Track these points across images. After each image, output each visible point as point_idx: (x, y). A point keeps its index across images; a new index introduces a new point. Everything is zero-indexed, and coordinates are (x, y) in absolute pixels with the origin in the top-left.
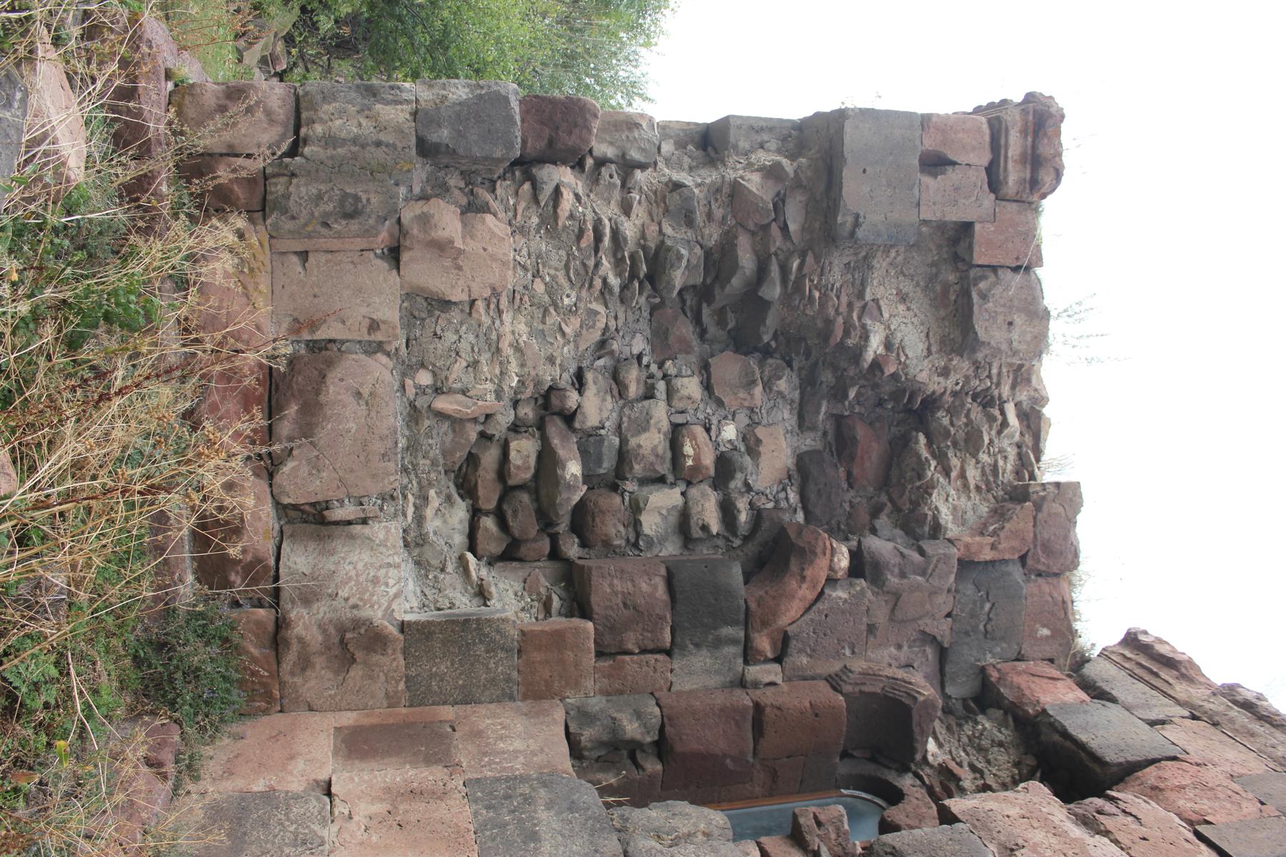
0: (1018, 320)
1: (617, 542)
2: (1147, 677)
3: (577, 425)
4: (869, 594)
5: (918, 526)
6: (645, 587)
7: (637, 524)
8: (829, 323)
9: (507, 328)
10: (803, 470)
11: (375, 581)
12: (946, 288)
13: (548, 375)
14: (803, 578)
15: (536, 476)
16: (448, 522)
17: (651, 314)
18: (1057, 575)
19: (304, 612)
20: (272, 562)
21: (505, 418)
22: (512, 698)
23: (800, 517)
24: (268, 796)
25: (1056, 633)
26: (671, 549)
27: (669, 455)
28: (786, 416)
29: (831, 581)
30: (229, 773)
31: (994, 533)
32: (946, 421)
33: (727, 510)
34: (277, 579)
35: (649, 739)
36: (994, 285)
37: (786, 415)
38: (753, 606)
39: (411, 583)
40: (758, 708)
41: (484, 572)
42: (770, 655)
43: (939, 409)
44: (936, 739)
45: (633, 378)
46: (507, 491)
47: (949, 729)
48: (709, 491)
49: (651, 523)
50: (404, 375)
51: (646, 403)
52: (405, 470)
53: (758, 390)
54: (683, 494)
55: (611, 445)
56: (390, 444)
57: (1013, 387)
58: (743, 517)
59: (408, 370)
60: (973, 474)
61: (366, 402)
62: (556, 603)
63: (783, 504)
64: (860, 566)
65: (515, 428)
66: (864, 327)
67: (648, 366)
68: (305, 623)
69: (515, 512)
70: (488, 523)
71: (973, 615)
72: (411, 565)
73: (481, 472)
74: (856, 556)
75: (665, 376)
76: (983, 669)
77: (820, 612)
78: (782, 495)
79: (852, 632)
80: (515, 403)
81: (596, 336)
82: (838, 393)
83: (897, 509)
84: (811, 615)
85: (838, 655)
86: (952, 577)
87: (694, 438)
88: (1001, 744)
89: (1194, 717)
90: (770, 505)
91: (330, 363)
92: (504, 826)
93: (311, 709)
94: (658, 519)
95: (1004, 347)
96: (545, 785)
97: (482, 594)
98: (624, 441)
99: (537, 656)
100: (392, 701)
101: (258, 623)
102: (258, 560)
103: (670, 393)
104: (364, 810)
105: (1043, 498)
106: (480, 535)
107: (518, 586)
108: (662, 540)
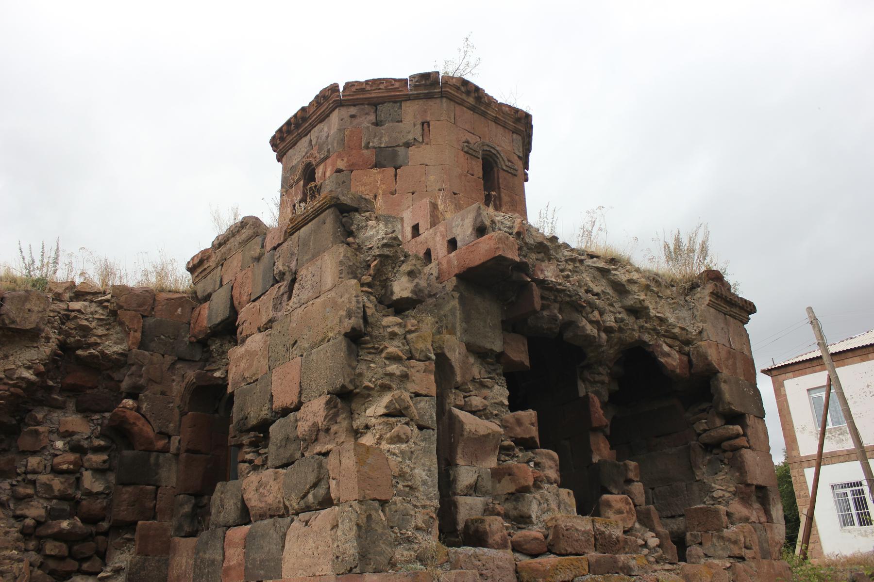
0: (28, 306)
1: (105, 504)
2: (206, 273)
3: (43, 520)
4: (146, 393)
5: (121, 362)
6: (126, 496)
7: (98, 493)
8: (12, 394)
10: (84, 410)
14: (134, 423)
15: (65, 542)
18: (155, 300)
22: (167, 560)
23: (107, 415)
26: (112, 478)
27: (66, 476)
28: (56, 415)
31: (130, 329)
32: (72, 339)
33: (98, 450)
35: (193, 501)
36: (9, 317)
37: (56, 414)
38: (143, 448)
40: (187, 451)
41: (109, 569)
42: (166, 441)
43: (65, 340)
44: (215, 370)
46: (71, 555)
47: (214, 362)
48: (87, 457)
49: (98, 487)
51: (38, 485)
53: (41, 429)
57: (61, 301)
58: (102, 443)
60: (100, 331)
62: (128, 536)
63: (100, 421)
64: (134, 395)
66: (17, 378)
70: (85, 566)
74: (129, 396)
75: (26, 473)
76: (191, 343)
78: (95, 422)
79: (158, 409)
82: (50, 389)
84: (152, 422)
86: (146, 353)
87: (60, 464)
88: (221, 345)
89: (222, 265)
90: (99, 428)
92: (208, 572)
94: (97, 483)
95: (40, 315)
96: (198, 553)
97: (118, 571)
98: (55, 497)
103: (34, 472)
105: (117, 304)
106: (90, 570)
107: (118, 552)
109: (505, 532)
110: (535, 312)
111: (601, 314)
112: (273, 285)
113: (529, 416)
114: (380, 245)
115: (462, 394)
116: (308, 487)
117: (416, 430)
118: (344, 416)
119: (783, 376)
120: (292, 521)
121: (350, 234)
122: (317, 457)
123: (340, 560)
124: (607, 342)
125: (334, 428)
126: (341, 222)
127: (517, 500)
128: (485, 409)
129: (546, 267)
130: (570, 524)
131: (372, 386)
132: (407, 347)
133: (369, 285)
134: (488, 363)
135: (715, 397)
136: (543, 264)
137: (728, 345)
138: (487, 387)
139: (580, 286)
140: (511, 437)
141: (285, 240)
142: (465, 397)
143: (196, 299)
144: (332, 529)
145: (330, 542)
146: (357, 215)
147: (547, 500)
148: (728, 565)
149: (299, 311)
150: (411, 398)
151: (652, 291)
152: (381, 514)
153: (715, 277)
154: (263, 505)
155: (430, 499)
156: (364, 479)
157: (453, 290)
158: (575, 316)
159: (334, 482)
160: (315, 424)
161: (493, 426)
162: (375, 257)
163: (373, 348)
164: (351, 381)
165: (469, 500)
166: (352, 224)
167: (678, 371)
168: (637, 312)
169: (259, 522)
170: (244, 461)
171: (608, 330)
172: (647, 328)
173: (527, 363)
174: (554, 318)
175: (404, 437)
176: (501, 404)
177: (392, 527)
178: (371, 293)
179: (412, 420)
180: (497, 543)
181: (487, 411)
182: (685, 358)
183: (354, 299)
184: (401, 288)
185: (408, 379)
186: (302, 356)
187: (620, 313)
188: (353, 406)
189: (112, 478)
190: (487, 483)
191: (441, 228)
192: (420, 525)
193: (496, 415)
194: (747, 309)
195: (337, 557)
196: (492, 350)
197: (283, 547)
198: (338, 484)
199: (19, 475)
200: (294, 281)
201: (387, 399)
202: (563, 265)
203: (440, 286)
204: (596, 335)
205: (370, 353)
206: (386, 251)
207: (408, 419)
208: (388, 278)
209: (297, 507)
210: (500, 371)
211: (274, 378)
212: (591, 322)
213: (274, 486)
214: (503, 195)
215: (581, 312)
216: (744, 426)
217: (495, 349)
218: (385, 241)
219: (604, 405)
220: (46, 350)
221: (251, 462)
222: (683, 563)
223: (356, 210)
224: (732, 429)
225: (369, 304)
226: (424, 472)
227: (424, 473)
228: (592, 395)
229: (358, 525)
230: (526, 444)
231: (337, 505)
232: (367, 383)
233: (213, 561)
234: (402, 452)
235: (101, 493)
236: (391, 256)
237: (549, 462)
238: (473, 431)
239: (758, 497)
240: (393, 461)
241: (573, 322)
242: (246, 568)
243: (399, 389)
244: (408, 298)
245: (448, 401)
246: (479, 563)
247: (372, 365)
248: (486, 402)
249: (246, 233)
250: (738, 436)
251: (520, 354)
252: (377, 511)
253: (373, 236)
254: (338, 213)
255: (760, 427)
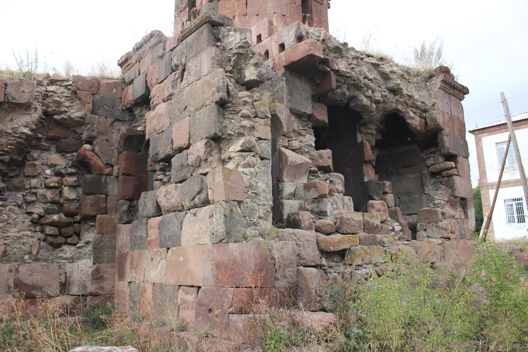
0: (22, 89)
1: (77, 206)
3: (43, 215)
4: (97, 140)
5: (81, 122)
6: (89, 201)
7: (73, 200)
8: (18, 143)
9: (13, 234)
10: (61, 151)
11: (82, 271)
12: (9, 107)
13: (28, 223)
14: (91, 159)
16: (68, 251)
17: (10, 191)
18: (99, 84)
19: (88, 289)
20: (75, 297)
21: (40, 235)
22: (115, 237)
23: (75, 154)
24: (130, 296)
25: (115, 87)
26: (80, 190)
27: (54, 190)
28: (45, 155)
29: (93, 151)
30: (125, 306)
33: (71, 174)
34: (79, 296)
35: (128, 203)
38: (97, 173)
39: (84, 261)
40: (124, 174)
41: (82, 242)
42: (111, 169)
43: (47, 110)
45: (30, 198)
46: (61, 234)
47: (137, 121)
48: (65, 179)
50: (25, 263)
51: (38, 195)
52: (52, 263)
53: (36, 163)
54: (65, 186)
55: (50, 206)
56: (45, 267)
57: (42, 86)
58: (73, 170)
59: (24, 262)
60: (67, 104)
61: (32, 273)
62: (92, 224)
63: (71, 158)
64: (90, 142)
65: (42, 231)
66: (20, 133)
67: (26, 193)
68: (91, 288)
69: (67, 233)
70: (69, 240)
71: (107, 111)
72: (79, 261)
73: (54, 242)
75: (30, 188)
76: (122, 110)
77: (101, 154)
78: (68, 158)
79: (106, 150)
80: (35, 232)
81: (16, 208)
82: (40, 139)
83: (76, 126)
85: (113, 150)
86: (96, 116)
87: (49, 183)
89: (140, 61)
90: (71, 162)
91: (21, 283)
93: (114, 287)
94: (72, 194)
95: (30, 94)
97: (87, 243)
98: (49, 202)
99: (105, 230)
100: (113, 267)
101: (90, 300)
102: (74, 300)
103: (35, 188)
104: (134, 275)
105: (76, 87)
106: (72, 242)
107: (87, 233)
108: (78, 193)
109: (311, 220)
110: (332, 90)
111: (373, 92)
112: (171, 73)
113: (327, 153)
114: (237, 47)
115: (287, 139)
116: (195, 193)
117: (259, 160)
118: (216, 151)
119: (482, 135)
120: (186, 213)
121: (218, 40)
122: (200, 176)
123: (214, 235)
124: (376, 109)
125: (210, 159)
126: (213, 33)
127: (319, 202)
128: (301, 148)
129: (340, 62)
130: (350, 216)
131: (233, 133)
132: (254, 110)
133: (230, 72)
134: (303, 121)
135: (440, 145)
136: (338, 60)
137: (450, 113)
138: (302, 135)
139: (361, 75)
140: (316, 165)
141: (178, 45)
142: (289, 141)
143: (126, 83)
144: (210, 218)
145: (209, 225)
146: (222, 28)
147: (336, 202)
148: (440, 242)
149: (188, 88)
150: (256, 141)
151: (405, 78)
152: (239, 209)
153: (445, 71)
154: (169, 205)
155: (267, 201)
156: (228, 189)
157: (282, 76)
158: (357, 93)
159: (211, 190)
160: (199, 157)
161: (305, 159)
162: (234, 55)
163: (233, 110)
164: (220, 131)
165: (290, 202)
166: (219, 34)
167: (418, 128)
168: (395, 91)
169: (167, 215)
170: (157, 180)
171: (377, 102)
172: (400, 101)
173: (327, 121)
174: (344, 94)
175: (252, 164)
176: (311, 146)
177: (245, 217)
178: (231, 77)
179: (257, 154)
180: (306, 227)
181: (302, 150)
182: (423, 121)
183: (221, 81)
184: (250, 74)
185: (254, 129)
186: (190, 116)
187: (384, 92)
188: (221, 145)
189: (80, 190)
190: (301, 192)
191: (275, 37)
192: (261, 216)
193: (307, 152)
194: (464, 91)
195: (213, 234)
196: (305, 113)
197: (181, 228)
198: (213, 192)
199: (27, 189)
200: (184, 70)
201: (241, 141)
202: (350, 61)
203: (274, 73)
204: (369, 105)
205: (231, 114)
206: (241, 51)
207: (254, 153)
208: (242, 68)
209: (189, 205)
210: (310, 126)
211: (174, 130)
212: (367, 97)
213: (175, 194)
214: (314, 17)
215: (361, 91)
216: (456, 162)
217: (307, 112)
218: (240, 44)
219: (372, 148)
220: (35, 116)
221: (161, 180)
222: (414, 241)
223: (222, 25)
224: (449, 164)
225: (230, 84)
226: (264, 185)
227: (264, 186)
228: (365, 141)
229: (225, 215)
230: (325, 170)
231: (212, 204)
232: (229, 132)
233: (141, 237)
234: (251, 173)
235: (75, 199)
236: (243, 54)
237: (338, 180)
238: (293, 161)
239: (461, 204)
240: (246, 178)
241: (356, 96)
242: (160, 241)
243: (249, 135)
244: (254, 80)
245: (279, 143)
246: (296, 238)
247: (232, 121)
248: (301, 144)
249: (153, 41)
250: (452, 168)
251: (322, 115)
252: (236, 207)
253: (233, 41)
254: (211, 27)
255: (466, 164)
